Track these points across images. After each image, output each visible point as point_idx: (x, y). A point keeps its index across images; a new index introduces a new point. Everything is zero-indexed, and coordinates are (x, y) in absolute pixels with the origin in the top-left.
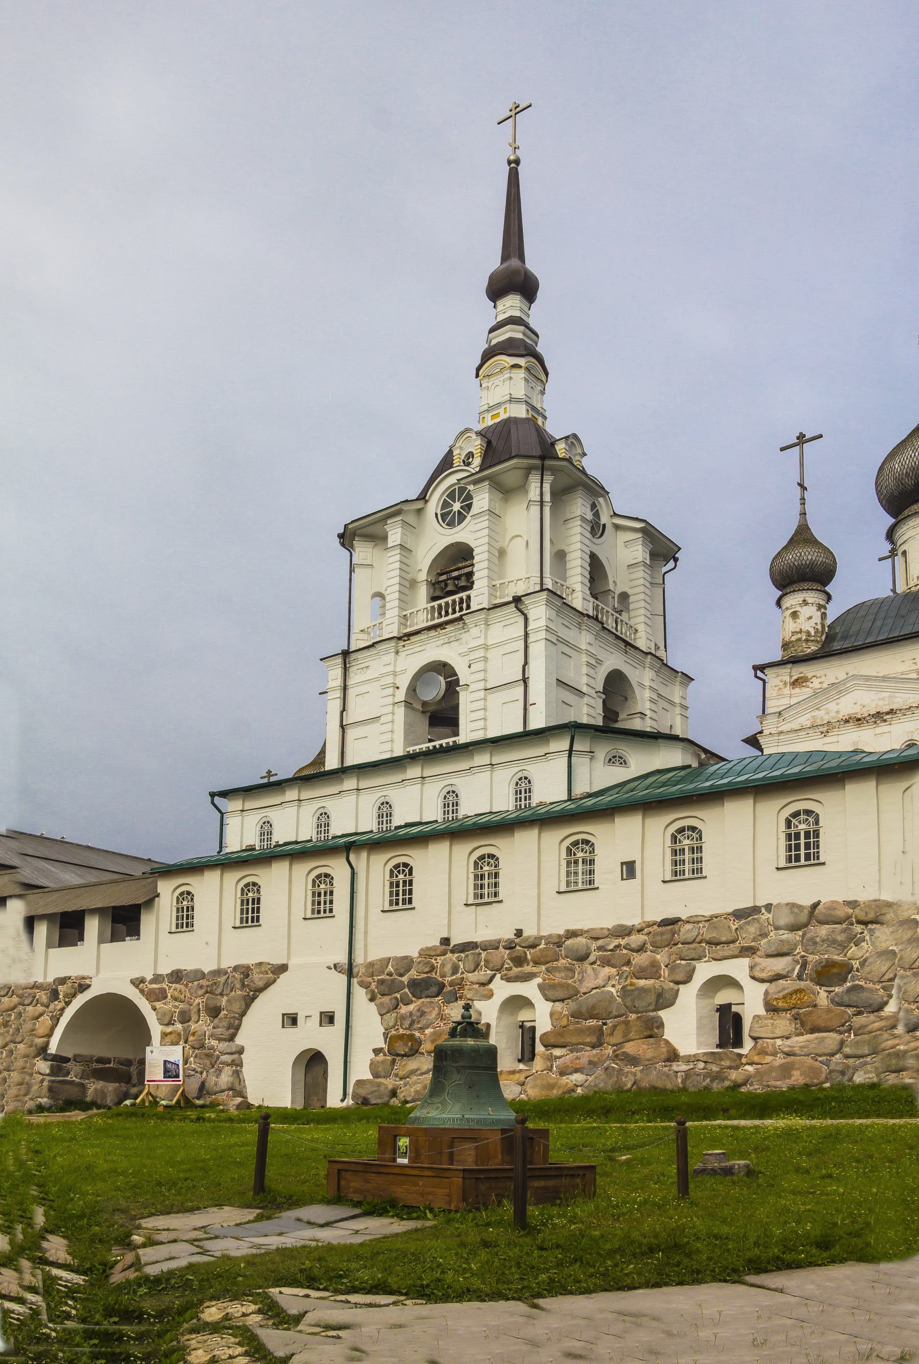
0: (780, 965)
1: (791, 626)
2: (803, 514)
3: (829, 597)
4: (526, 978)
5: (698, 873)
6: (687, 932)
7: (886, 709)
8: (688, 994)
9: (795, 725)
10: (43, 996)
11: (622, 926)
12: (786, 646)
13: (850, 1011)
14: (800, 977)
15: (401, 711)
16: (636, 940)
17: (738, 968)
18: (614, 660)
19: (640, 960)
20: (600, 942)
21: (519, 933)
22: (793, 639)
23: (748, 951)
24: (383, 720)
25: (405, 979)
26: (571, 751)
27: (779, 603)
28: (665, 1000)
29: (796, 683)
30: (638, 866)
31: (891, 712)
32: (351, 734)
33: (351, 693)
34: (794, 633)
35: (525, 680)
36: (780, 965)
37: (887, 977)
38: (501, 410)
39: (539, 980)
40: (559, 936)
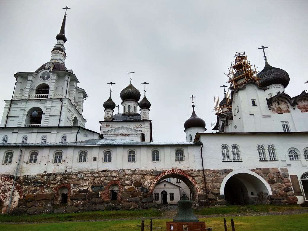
1: (107, 115)
2: (110, 96)
3: (114, 111)
5: (110, 161)
7: (128, 133)
9: (110, 134)
12: (105, 118)
18: (76, 115)
22: (107, 117)
26: (78, 132)
27: (104, 111)
29: (107, 126)
30: (97, 159)
31: (129, 134)
34: (107, 117)
35: (60, 115)
38: (57, 61)
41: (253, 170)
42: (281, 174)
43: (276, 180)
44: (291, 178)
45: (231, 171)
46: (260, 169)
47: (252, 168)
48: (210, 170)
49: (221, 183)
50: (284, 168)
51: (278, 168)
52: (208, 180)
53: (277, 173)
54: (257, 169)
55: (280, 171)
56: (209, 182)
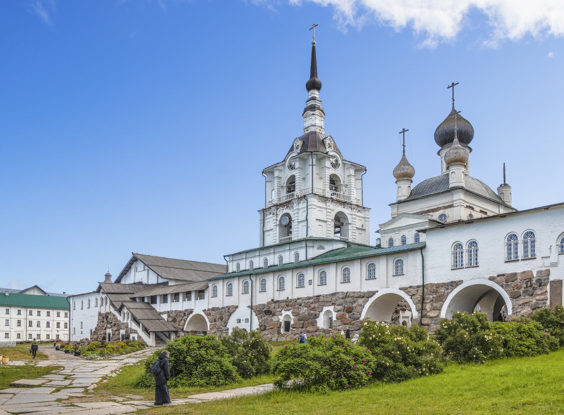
0: (339, 308)
4: (288, 310)
6: (321, 299)
8: (322, 314)
10: (182, 315)
11: (308, 297)
13: (352, 319)
14: (343, 311)
15: (278, 227)
16: (311, 301)
17: (331, 308)
19: (312, 306)
20: (304, 301)
21: (288, 298)
23: (333, 304)
24: (274, 230)
25: (264, 310)
26: (306, 246)
28: (316, 316)
32: (266, 234)
33: (266, 221)
35: (307, 220)
36: (339, 308)
37: (360, 311)
39: (292, 311)
40: (296, 299)
41: (492, 279)
42: (534, 281)
43: (524, 292)
44: (551, 286)
45: (461, 282)
46: (503, 275)
47: (492, 275)
48: (432, 285)
49: (444, 302)
50: (543, 269)
51: (533, 271)
52: (427, 299)
53: (527, 280)
54: (498, 276)
55: (535, 275)
56: (428, 301)
